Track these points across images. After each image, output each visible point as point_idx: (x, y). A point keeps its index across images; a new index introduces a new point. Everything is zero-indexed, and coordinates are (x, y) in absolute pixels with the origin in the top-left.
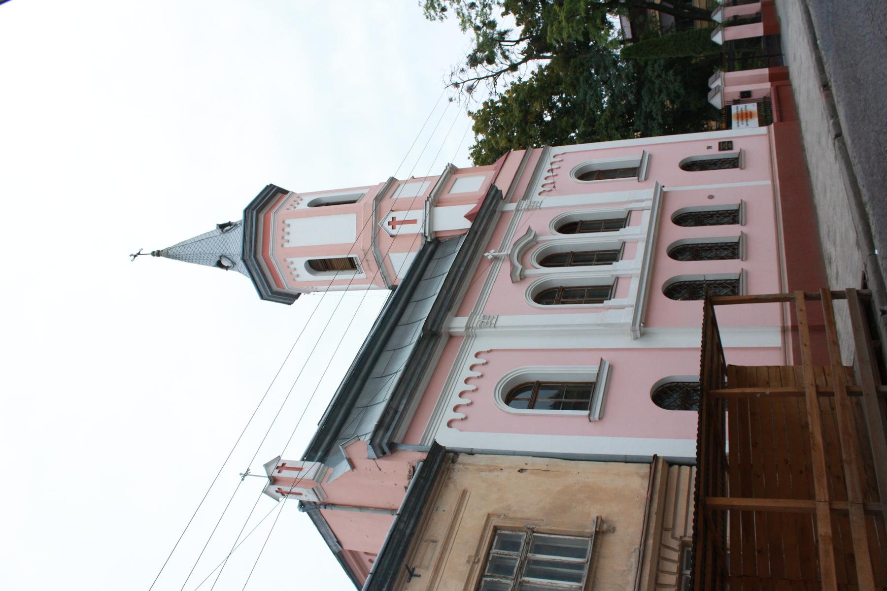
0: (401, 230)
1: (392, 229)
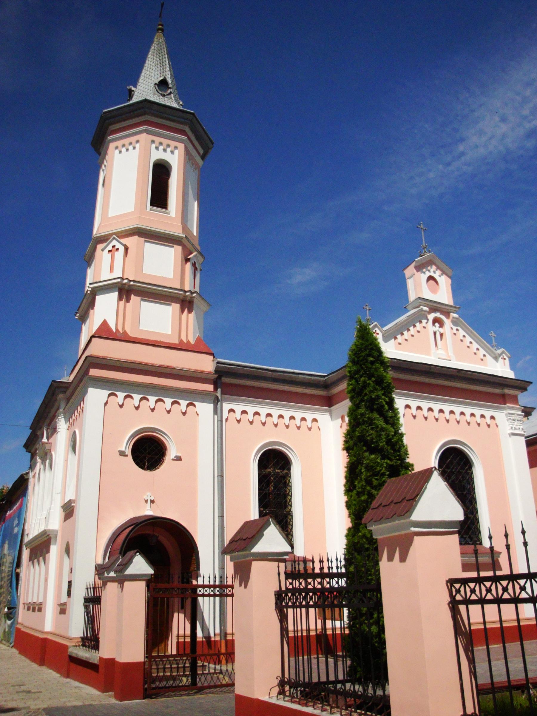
1: (110, 251)
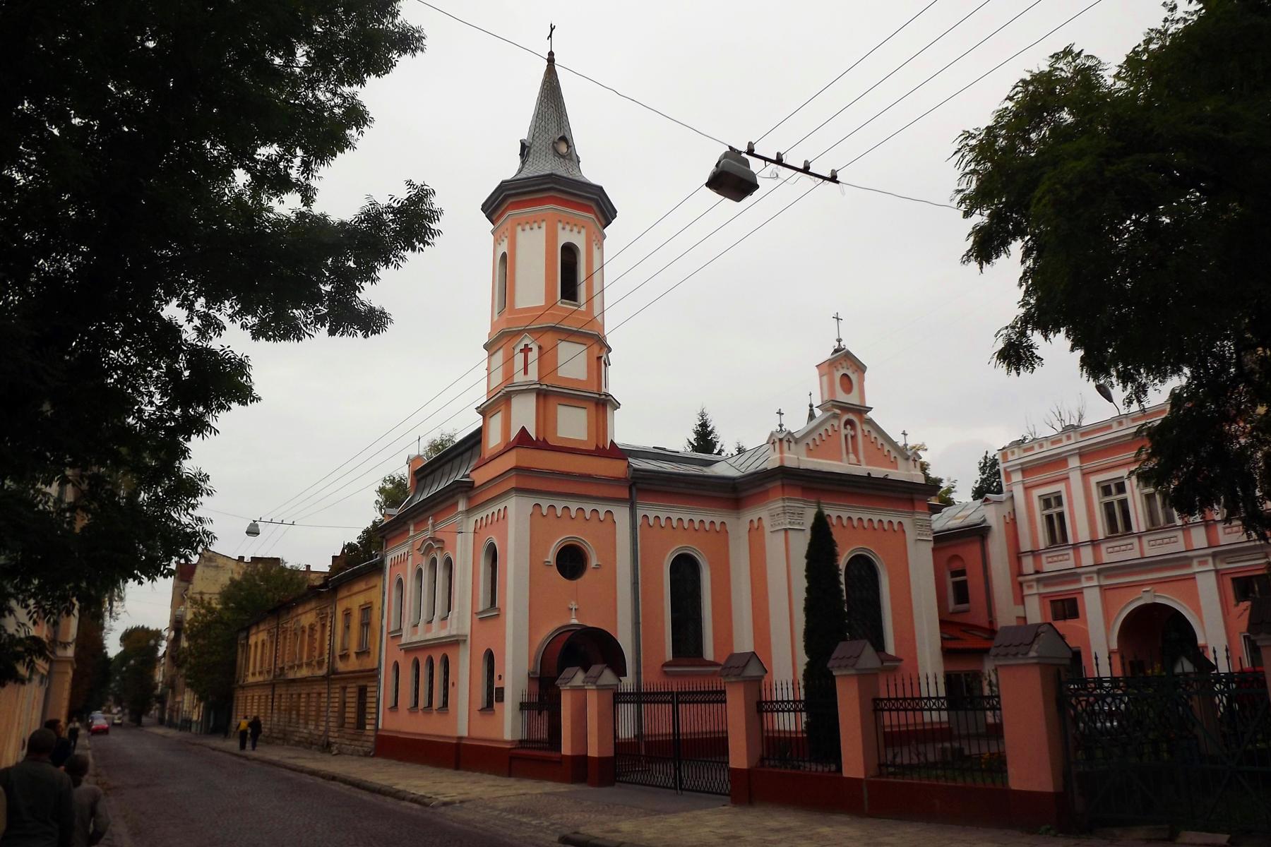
0: (519, 359)
1: (521, 351)
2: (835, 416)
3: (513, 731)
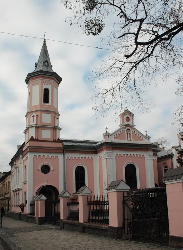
0: (32, 118)
1: (32, 117)
2: (123, 128)
3: (28, 211)
